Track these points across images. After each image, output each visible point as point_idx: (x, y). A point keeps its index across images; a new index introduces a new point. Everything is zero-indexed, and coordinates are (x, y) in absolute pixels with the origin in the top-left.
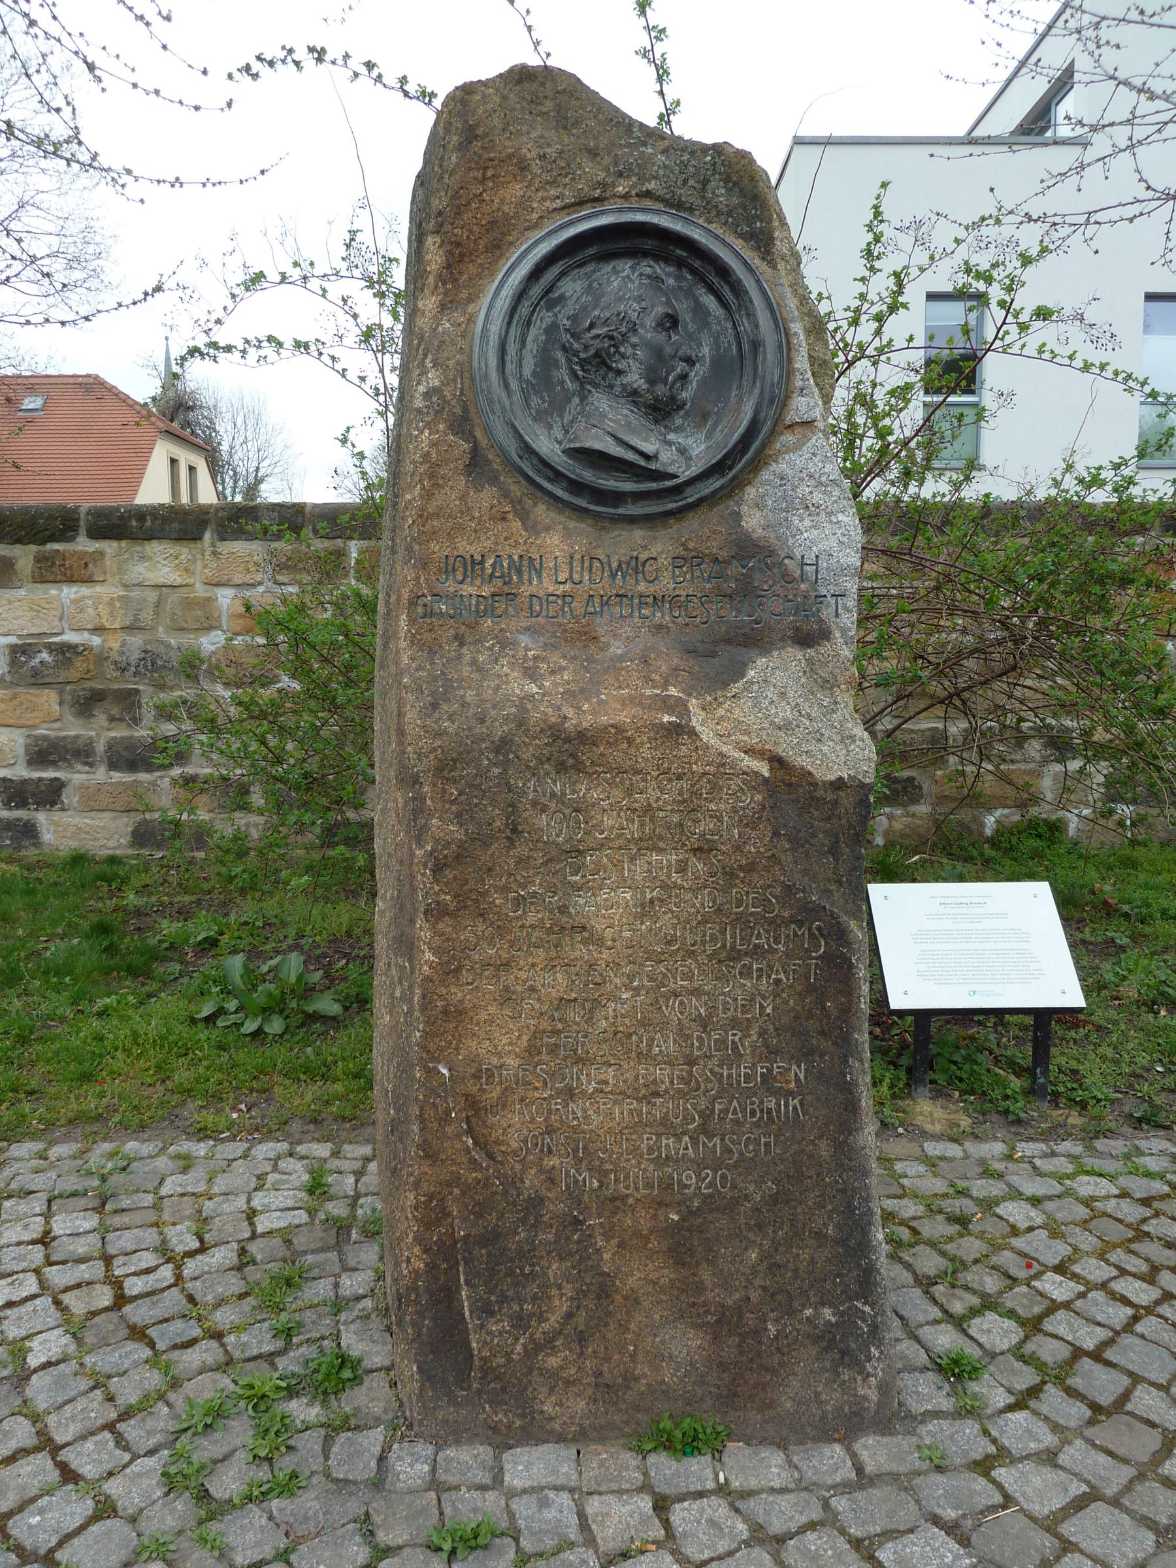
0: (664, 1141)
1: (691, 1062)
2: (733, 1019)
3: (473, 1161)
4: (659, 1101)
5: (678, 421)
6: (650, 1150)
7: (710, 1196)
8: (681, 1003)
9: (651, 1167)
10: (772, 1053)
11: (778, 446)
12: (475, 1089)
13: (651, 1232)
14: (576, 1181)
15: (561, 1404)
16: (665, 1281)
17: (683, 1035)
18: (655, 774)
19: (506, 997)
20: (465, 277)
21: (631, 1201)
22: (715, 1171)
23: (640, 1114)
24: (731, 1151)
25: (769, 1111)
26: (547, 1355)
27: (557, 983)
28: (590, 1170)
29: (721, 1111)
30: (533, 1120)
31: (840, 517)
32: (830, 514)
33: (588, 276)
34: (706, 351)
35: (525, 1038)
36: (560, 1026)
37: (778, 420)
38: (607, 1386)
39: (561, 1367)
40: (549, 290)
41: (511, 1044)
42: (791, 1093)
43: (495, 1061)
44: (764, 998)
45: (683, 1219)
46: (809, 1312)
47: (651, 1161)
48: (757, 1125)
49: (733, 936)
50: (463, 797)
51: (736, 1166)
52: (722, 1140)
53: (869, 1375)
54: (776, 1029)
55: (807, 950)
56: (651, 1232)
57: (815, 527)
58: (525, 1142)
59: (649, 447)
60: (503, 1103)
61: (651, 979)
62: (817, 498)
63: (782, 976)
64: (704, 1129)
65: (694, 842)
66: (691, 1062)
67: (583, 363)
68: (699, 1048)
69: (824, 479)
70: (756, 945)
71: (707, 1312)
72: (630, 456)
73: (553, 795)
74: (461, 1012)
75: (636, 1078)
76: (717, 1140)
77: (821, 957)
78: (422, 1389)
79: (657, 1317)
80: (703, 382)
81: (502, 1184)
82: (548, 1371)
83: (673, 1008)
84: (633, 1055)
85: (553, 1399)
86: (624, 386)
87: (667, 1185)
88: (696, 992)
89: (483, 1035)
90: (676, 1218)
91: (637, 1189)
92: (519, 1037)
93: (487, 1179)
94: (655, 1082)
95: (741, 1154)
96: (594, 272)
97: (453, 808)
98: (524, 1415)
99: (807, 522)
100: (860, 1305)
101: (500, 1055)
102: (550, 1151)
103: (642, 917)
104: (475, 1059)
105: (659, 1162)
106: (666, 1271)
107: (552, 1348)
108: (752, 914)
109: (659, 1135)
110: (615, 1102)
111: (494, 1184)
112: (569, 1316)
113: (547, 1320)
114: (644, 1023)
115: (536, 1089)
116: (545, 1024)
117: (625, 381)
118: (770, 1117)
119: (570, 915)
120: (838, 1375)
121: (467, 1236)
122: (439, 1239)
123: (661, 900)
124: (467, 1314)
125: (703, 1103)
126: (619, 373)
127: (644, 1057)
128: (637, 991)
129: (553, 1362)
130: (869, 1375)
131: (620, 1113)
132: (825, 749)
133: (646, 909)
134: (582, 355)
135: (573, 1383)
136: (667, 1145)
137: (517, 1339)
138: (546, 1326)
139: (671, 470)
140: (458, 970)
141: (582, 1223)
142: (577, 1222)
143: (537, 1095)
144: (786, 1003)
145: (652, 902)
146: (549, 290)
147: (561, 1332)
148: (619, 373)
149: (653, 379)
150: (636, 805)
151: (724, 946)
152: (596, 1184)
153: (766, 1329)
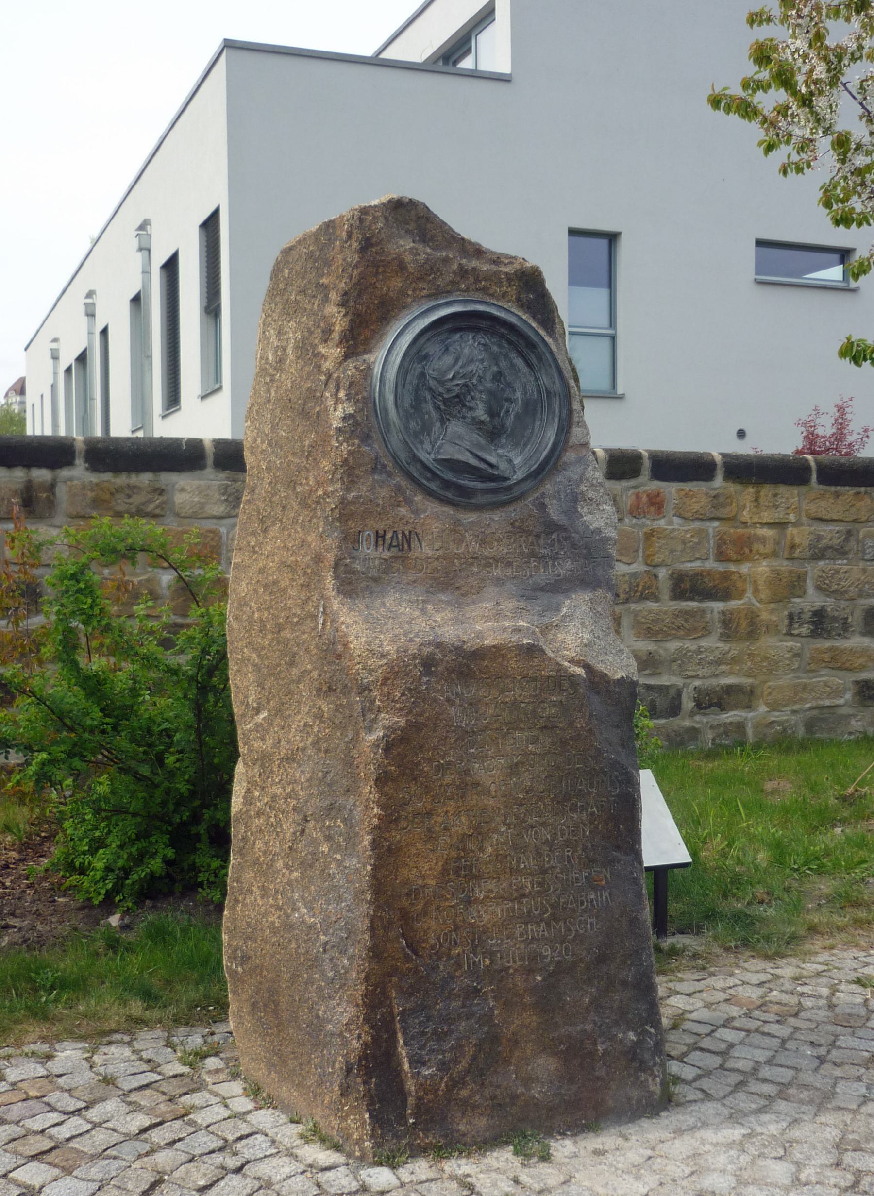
0: (530, 927)
1: (544, 872)
2: (568, 841)
3: (406, 956)
4: (525, 900)
5: (503, 441)
6: (521, 935)
7: (559, 962)
8: (536, 833)
9: (523, 946)
10: (592, 861)
11: (565, 459)
12: (407, 904)
13: (525, 991)
14: (474, 962)
15: (470, 1123)
16: (534, 1024)
17: (539, 854)
18: (519, 678)
19: (430, 836)
20: (362, 337)
21: (511, 971)
22: (562, 943)
23: (513, 910)
24: (570, 930)
25: (592, 901)
26: (460, 1089)
27: (462, 825)
28: (483, 953)
29: (564, 903)
30: (445, 921)
31: (604, 506)
32: (598, 505)
33: (443, 341)
34: (518, 394)
35: (440, 864)
36: (462, 854)
37: (566, 441)
38: (500, 1105)
39: (470, 1096)
40: (420, 350)
41: (430, 869)
42: (603, 887)
43: (420, 882)
44: (584, 825)
45: (544, 980)
46: (620, 1035)
47: (521, 941)
48: (584, 911)
49: (567, 785)
50: (404, 698)
51: (574, 940)
52: (565, 923)
53: (656, 1076)
54: (593, 846)
55: (610, 791)
56: (525, 991)
57: (590, 513)
58: (439, 939)
59: (493, 460)
60: (425, 913)
61: (517, 818)
62: (591, 494)
63: (595, 809)
64: (555, 918)
65: (542, 723)
66: (544, 872)
67: (445, 401)
68: (549, 862)
69: (595, 482)
70: (580, 790)
71: (561, 1043)
72: (483, 466)
73: (457, 694)
74: (399, 849)
75: (511, 885)
76: (562, 923)
77: (617, 796)
78: (373, 1130)
79: (529, 1052)
80: (518, 417)
81: (425, 970)
82: (461, 1100)
83: (531, 836)
84: (508, 870)
85: (464, 1121)
86: (473, 418)
87: (533, 957)
88: (544, 824)
89: (412, 864)
90: (540, 979)
91: (514, 962)
92: (436, 864)
93: (416, 967)
94: (522, 887)
95: (577, 931)
96: (447, 339)
97: (398, 705)
98: (445, 1136)
99: (585, 510)
100: (648, 1028)
101: (423, 877)
102: (456, 943)
103: (510, 775)
104: (406, 883)
105: (528, 942)
106: (534, 1018)
107: (463, 1084)
108: (578, 769)
109: (526, 924)
110: (497, 905)
111: (420, 971)
112: (474, 1058)
113: (460, 1062)
114: (515, 847)
115: (447, 899)
116: (454, 854)
117: (474, 415)
118: (593, 905)
119: (471, 777)
120: (638, 1078)
121: (404, 1011)
122: (382, 1016)
123: (523, 763)
124: (406, 1067)
125: (554, 898)
126: (471, 409)
127: (515, 872)
128: (509, 825)
129: (464, 1093)
130: (656, 1076)
131: (499, 911)
132: (611, 659)
133: (514, 769)
134: (446, 396)
135: (478, 1107)
136: (532, 930)
137: (442, 1079)
138: (460, 1067)
139: (506, 475)
140: (397, 820)
141: (480, 990)
142: (477, 991)
143: (447, 904)
144: (597, 828)
145: (517, 764)
146: (420, 350)
147: (469, 1072)
148: (471, 409)
149: (492, 413)
150: (507, 700)
151: (561, 792)
152: (488, 962)
153: (597, 1050)
